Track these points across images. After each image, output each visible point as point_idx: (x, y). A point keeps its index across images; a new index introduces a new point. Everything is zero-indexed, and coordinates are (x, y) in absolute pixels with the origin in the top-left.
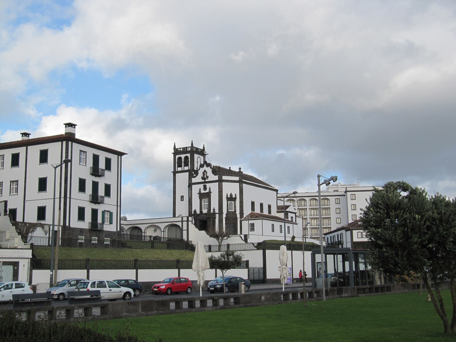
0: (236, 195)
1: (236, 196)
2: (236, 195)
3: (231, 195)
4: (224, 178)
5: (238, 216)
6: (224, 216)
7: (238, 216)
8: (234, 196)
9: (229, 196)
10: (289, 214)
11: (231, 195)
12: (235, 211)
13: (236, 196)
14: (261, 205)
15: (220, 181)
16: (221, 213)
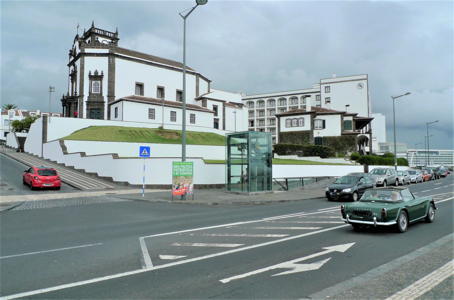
0: (102, 72)
1: (102, 74)
2: (102, 72)
3: (96, 72)
4: (87, 51)
5: (106, 99)
6: (85, 99)
7: (106, 99)
8: (100, 74)
9: (93, 74)
10: (208, 101)
11: (96, 72)
12: (101, 94)
13: (102, 74)
14: (161, 90)
15: (83, 55)
16: (82, 96)
